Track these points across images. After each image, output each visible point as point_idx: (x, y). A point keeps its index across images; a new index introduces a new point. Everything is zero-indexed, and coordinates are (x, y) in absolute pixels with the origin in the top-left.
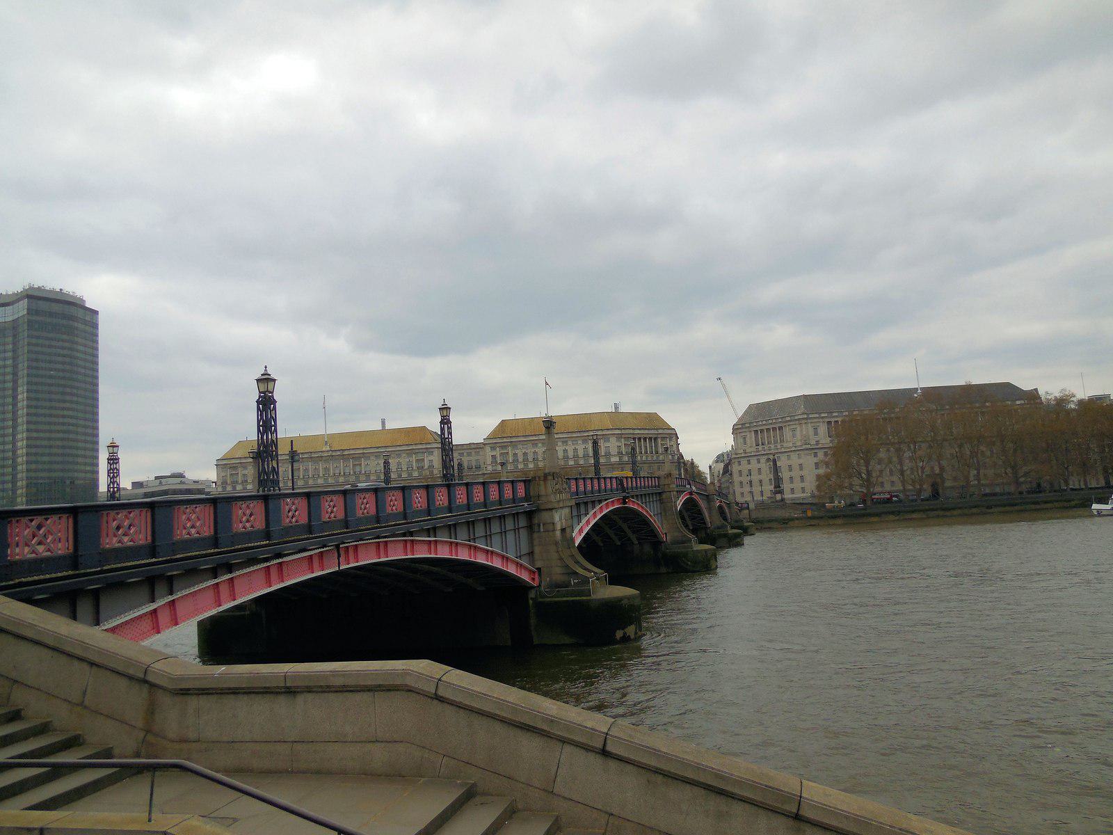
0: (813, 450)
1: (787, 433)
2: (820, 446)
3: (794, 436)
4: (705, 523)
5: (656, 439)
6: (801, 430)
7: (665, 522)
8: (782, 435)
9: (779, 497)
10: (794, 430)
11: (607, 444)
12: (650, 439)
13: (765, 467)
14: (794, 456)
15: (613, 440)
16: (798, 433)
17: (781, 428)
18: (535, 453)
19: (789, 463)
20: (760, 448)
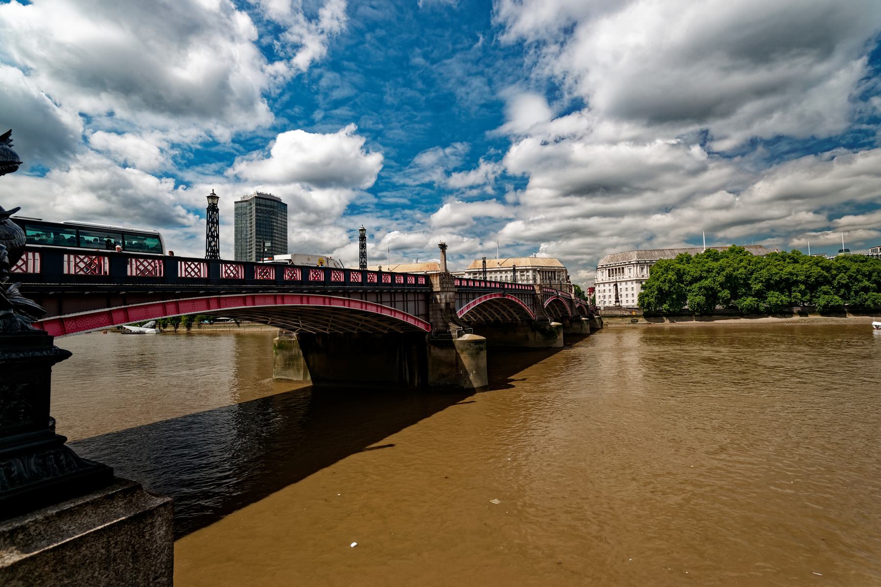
0: (639, 281)
1: (626, 270)
2: (644, 278)
3: (630, 272)
4: (568, 314)
5: (555, 272)
6: (634, 269)
7: (535, 309)
8: (623, 272)
9: (617, 304)
10: (630, 269)
11: (528, 274)
12: (552, 272)
13: (612, 287)
14: (629, 283)
15: (531, 271)
16: (632, 270)
17: (623, 268)
18: (491, 277)
19: (626, 286)
20: (611, 278)
